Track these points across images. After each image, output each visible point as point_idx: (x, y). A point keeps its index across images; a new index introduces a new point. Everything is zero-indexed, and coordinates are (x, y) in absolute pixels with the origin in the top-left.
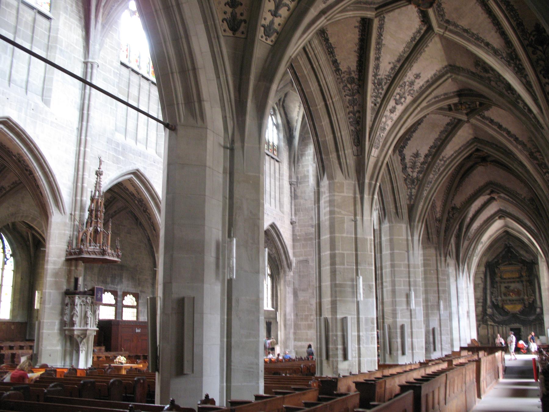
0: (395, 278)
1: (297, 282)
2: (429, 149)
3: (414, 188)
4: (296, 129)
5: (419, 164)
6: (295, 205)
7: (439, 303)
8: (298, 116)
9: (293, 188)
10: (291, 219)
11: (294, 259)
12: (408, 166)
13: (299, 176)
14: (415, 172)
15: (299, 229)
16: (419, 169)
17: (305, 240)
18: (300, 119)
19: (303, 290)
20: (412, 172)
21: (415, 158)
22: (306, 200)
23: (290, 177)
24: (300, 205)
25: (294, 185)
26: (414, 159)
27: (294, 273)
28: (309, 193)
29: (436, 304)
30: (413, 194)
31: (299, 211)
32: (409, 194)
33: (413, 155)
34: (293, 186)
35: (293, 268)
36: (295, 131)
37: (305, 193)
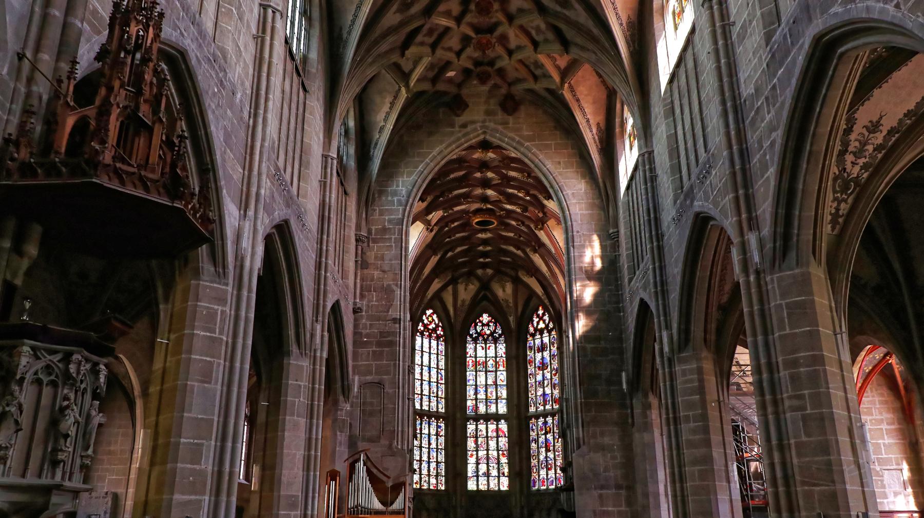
0: (828, 388)
1: (357, 424)
2: (901, 116)
3: (845, 201)
4: (376, 144)
5: (870, 148)
6: (362, 280)
7: (726, 466)
8: (386, 120)
9: (360, 248)
10: (355, 303)
11: (357, 378)
12: (851, 149)
13: (373, 228)
14: (857, 164)
15: (368, 323)
16: (867, 159)
17: (379, 344)
18: (390, 126)
19: (371, 440)
20: (852, 163)
21: (870, 132)
22: (384, 271)
23: (358, 227)
24: (372, 280)
25: (363, 242)
26: (867, 134)
27: (352, 406)
28: (391, 260)
29: (723, 468)
30: (841, 213)
31: (371, 291)
32: (833, 211)
33: (869, 124)
34: (360, 243)
35: (351, 397)
36: (375, 148)
37: (382, 259)
